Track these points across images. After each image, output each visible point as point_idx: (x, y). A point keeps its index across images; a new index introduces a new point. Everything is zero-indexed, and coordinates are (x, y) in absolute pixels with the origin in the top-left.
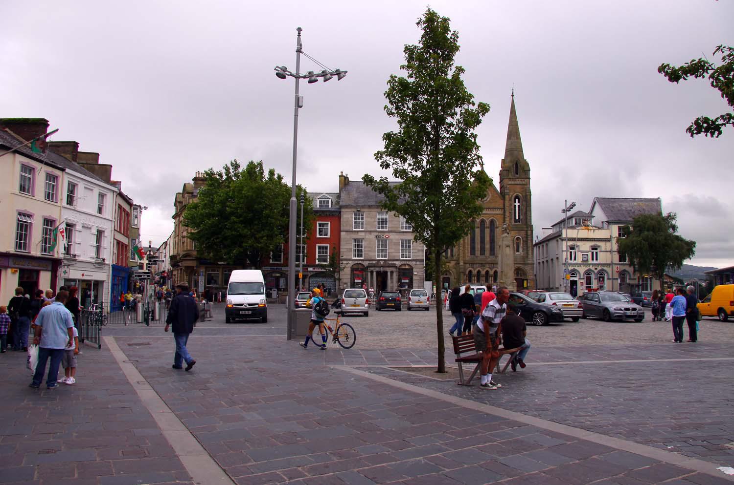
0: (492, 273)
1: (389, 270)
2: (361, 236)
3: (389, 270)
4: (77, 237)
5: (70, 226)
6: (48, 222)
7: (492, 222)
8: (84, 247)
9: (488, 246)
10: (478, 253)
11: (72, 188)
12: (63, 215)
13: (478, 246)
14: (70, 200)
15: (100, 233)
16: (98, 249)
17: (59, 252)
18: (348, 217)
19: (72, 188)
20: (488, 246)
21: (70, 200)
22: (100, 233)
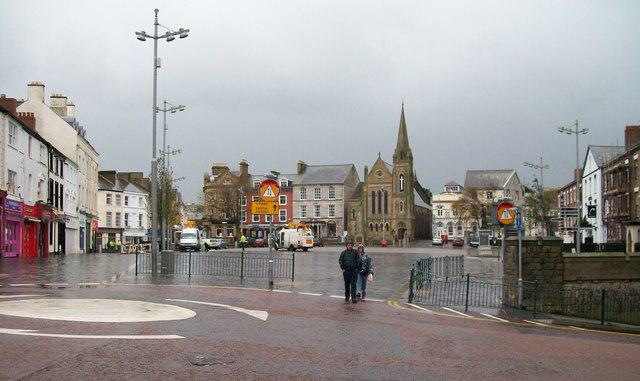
0: (385, 225)
1: (318, 225)
2: (305, 203)
3: (318, 225)
4: (130, 218)
5: (126, 215)
6: (118, 214)
7: (386, 193)
8: (134, 222)
9: (383, 208)
10: (377, 212)
11: (126, 198)
12: (124, 210)
13: (377, 208)
14: (126, 203)
15: (141, 216)
16: (140, 224)
17: (123, 225)
18: (297, 192)
19: (126, 198)
20: (383, 208)
21: (126, 203)
22: (141, 216)
